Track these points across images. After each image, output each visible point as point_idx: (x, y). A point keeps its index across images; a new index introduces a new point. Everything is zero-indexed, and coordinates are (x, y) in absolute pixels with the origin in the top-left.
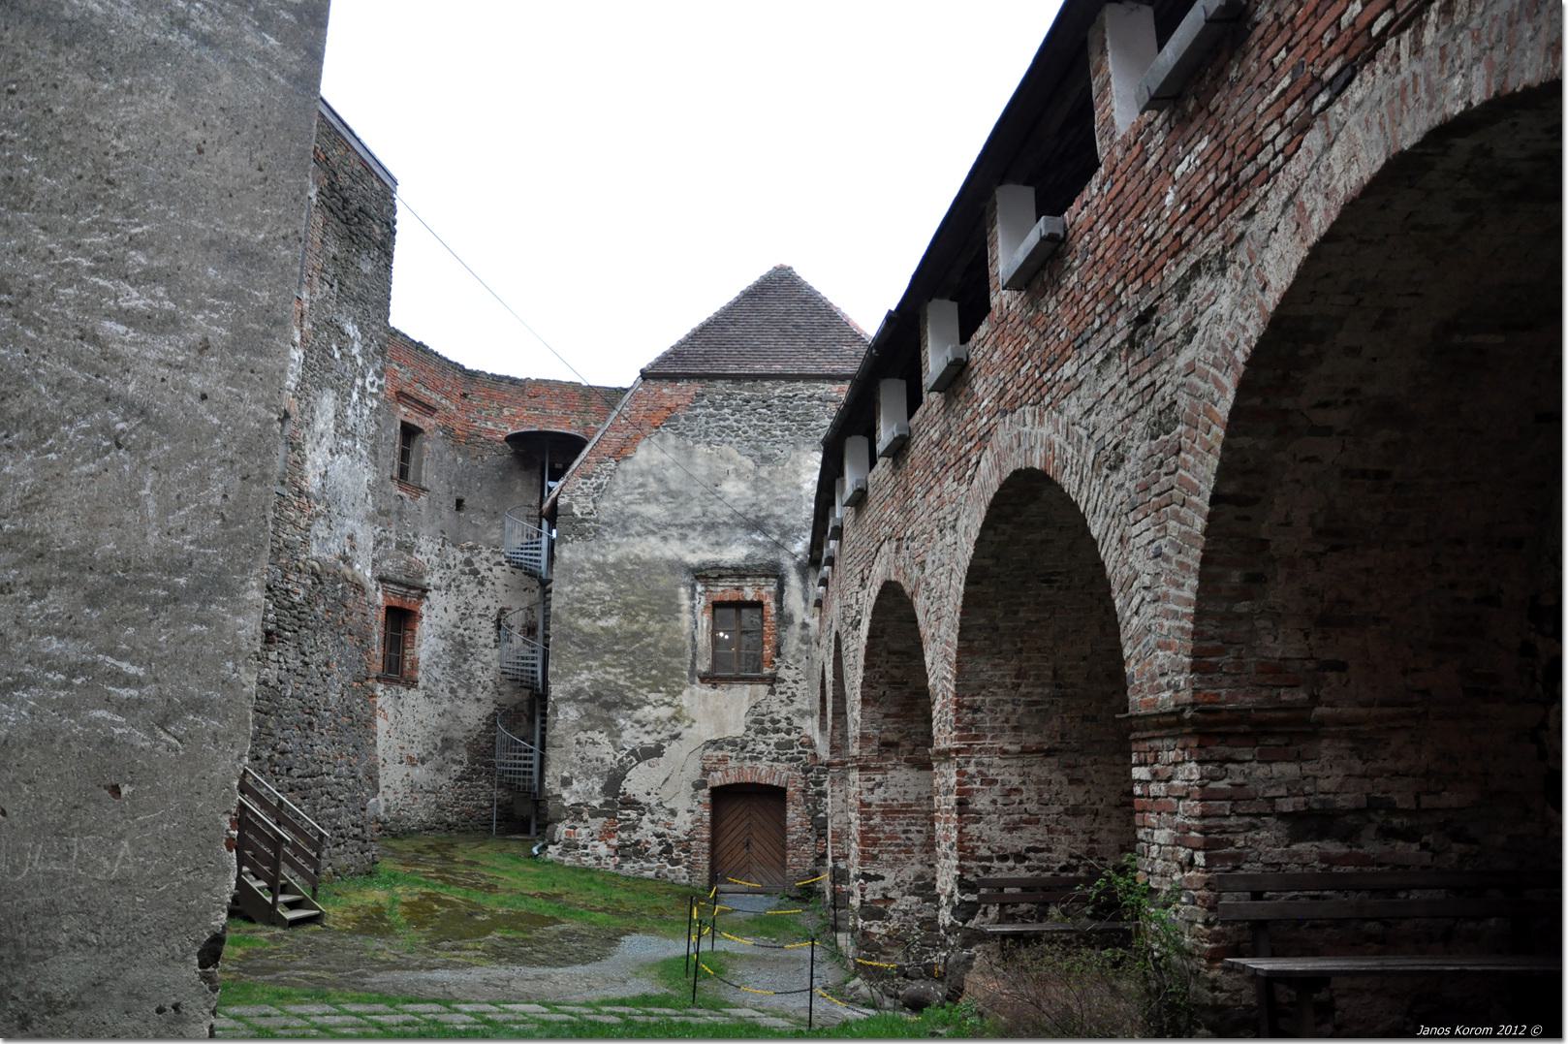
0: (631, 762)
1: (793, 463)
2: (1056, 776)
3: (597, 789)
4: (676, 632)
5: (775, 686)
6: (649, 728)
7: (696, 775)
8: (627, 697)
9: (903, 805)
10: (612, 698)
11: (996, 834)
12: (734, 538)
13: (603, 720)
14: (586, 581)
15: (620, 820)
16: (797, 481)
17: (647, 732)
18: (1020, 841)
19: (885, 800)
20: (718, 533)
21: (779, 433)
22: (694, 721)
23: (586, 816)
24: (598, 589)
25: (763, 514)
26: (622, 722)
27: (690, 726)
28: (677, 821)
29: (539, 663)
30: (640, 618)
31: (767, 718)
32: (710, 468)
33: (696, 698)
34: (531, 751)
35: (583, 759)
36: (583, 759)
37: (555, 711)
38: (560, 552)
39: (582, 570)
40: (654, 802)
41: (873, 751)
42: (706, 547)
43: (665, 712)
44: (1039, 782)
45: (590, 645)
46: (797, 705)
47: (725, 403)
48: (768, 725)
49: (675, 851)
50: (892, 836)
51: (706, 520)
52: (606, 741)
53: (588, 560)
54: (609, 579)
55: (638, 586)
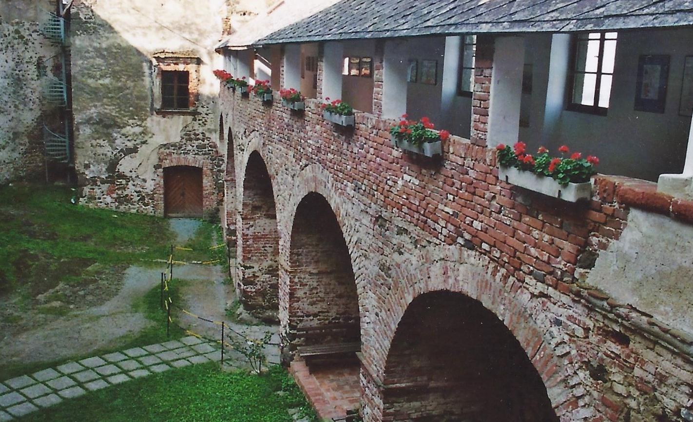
0: (121, 155)
2: (333, 282)
3: (104, 169)
4: (142, 87)
5: (196, 116)
6: (129, 138)
7: (156, 162)
8: (117, 122)
9: (263, 235)
10: (108, 122)
11: (306, 306)
13: (104, 133)
14: (90, 58)
15: (117, 185)
17: (128, 140)
18: (315, 309)
19: (255, 233)
22: (154, 134)
23: (99, 183)
24: (97, 63)
26: (115, 135)
28: (147, 185)
29: (64, 90)
30: (123, 80)
33: (154, 122)
34: (64, 142)
35: (95, 154)
36: (95, 154)
37: (78, 130)
38: (74, 41)
39: (88, 52)
40: (134, 175)
41: (249, 210)
43: (138, 130)
44: (326, 284)
45: (95, 94)
46: (207, 127)
48: (193, 136)
49: (146, 199)
50: (258, 249)
52: (107, 145)
53: (91, 46)
54: (103, 57)
55: (120, 61)
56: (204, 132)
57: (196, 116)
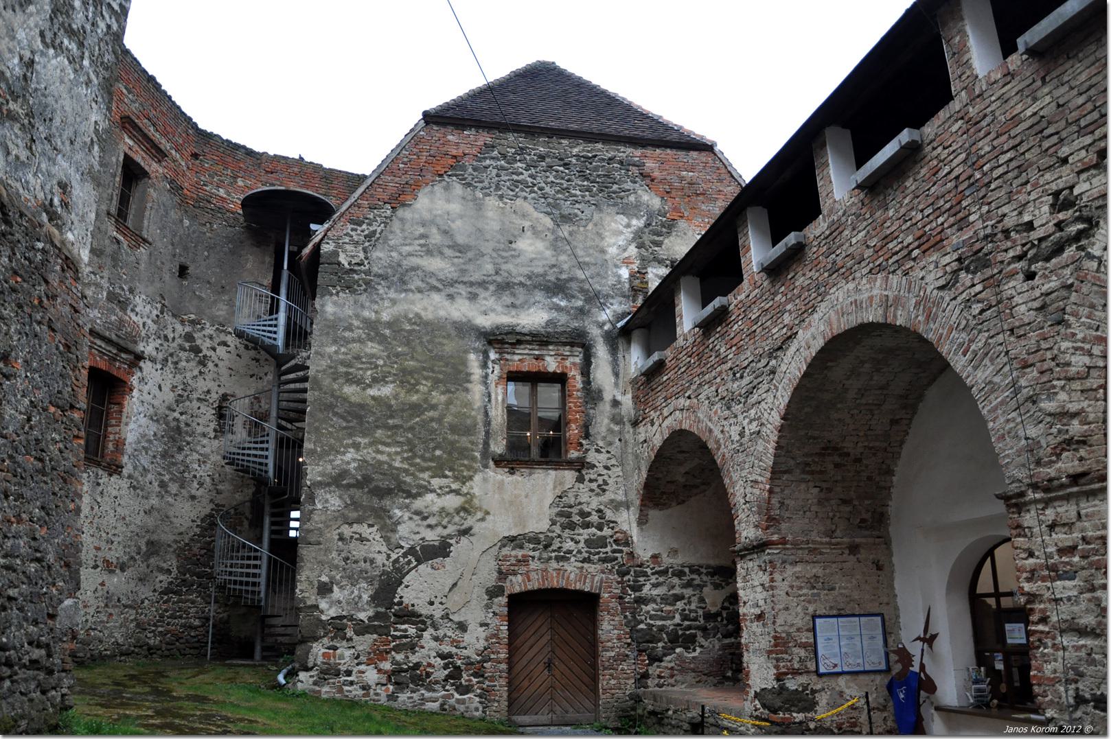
0: (409, 562)
1: (596, 225)
3: (366, 597)
6: (432, 521)
7: (491, 579)
8: (405, 482)
10: (385, 484)
12: (532, 300)
13: (373, 509)
14: (354, 341)
15: (395, 638)
16: (601, 245)
17: (429, 526)
20: (513, 295)
21: (578, 193)
22: (487, 513)
23: (350, 633)
24: (368, 350)
25: (564, 276)
26: (398, 513)
27: (483, 519)
28: (468, 638)
31: (575, 510)
32: (503, 223)
35: (347, 559)
38: (323, 306)
39: (349, 328)
40: (438, 613)
42: (499, 309)
43: (452, 502)
46: (609, 496)
47: (518, 158)
48: (576, 518)
51: (499, 279)
52: (377, 537)
53: (357, 316)
54: (382, 340)
55: (419, 349)
56: (602, 507)
57: (584, 472)
